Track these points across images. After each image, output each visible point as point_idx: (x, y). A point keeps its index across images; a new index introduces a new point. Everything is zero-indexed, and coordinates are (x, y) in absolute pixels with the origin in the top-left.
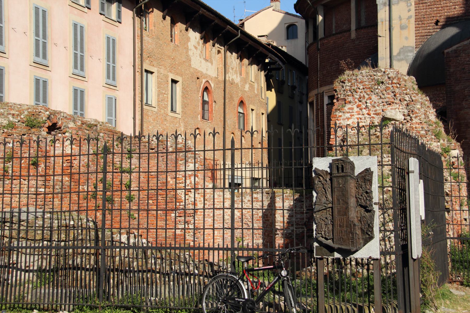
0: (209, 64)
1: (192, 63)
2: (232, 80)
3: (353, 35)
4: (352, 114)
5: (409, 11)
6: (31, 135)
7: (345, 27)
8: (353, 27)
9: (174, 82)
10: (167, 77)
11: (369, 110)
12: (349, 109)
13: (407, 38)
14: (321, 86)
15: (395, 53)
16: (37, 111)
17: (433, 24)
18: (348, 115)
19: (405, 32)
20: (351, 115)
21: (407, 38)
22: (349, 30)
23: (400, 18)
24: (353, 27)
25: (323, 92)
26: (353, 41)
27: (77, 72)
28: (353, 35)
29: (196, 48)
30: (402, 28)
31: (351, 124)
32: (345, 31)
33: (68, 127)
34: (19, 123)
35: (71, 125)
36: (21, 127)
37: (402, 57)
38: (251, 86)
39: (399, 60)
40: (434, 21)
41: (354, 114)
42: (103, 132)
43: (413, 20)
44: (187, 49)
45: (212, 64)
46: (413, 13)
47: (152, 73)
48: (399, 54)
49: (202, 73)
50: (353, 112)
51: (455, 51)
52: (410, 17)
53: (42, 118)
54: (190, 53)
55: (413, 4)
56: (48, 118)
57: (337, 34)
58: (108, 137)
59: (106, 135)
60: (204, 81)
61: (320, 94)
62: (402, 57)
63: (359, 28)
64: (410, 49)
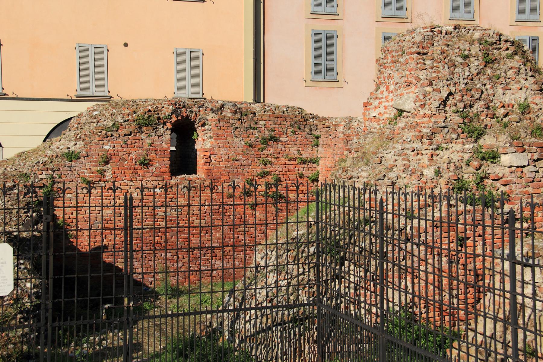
4: (381, 101)
6: (138, 135)
16: (159, 106)
20: (379, 104)
31: (377, 116)
33: (207, 120)
34: (126, 123)
35: (211, 116)
36: (129, 127)
41: (382, 100)
42: (266, 119)
50: (382, 98)
53: (165, 114)
56: (172, 113)
58: (274, 124)
59: (272, 123)
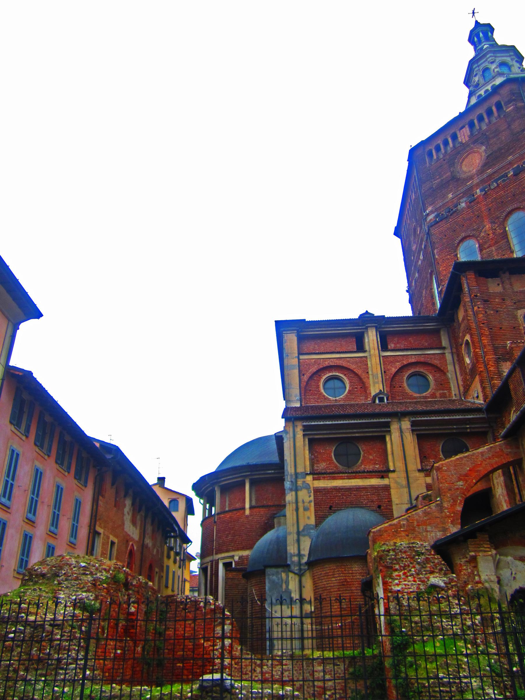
0: (135, 529)
1: (125, 526)
2: (147, 544)
3: (247, 512)
5: (310, 496)
7: (238, 505)
8: (247, 506)
9: (113, 543)
10: (108, 538)
11: (414, 578)
12: (397, 575)
13: (309, 518)
14: (216, 554)
15: (301, 528)
17: (328, 509)
18: (397, 581)
19: (307, 513)
22: (244, 508)
23: (303, 502)
24: (247, 506)
25: (218, 560)
26: (247, 517)
27: (53, 529)
28: (247, 512)
29: (128, 514)
30: (306, 509)
32: (240, 509)
38: (158, 551)
39: (304, 536)
43: (313, 504)
44: (123, 514)
45: (136, 528)
46: (312, 498)
47: (99, 534)
48: (303, 530)
49: (129, 535)
51: (380, 530)
52: (310, 502)
54: (125, 518)
55: (312, 492)
57: (230, 511)
60: (131, 543)
61: (215, 560)
62: (305, 533)
63: (251, 508)
64: (312, 526)
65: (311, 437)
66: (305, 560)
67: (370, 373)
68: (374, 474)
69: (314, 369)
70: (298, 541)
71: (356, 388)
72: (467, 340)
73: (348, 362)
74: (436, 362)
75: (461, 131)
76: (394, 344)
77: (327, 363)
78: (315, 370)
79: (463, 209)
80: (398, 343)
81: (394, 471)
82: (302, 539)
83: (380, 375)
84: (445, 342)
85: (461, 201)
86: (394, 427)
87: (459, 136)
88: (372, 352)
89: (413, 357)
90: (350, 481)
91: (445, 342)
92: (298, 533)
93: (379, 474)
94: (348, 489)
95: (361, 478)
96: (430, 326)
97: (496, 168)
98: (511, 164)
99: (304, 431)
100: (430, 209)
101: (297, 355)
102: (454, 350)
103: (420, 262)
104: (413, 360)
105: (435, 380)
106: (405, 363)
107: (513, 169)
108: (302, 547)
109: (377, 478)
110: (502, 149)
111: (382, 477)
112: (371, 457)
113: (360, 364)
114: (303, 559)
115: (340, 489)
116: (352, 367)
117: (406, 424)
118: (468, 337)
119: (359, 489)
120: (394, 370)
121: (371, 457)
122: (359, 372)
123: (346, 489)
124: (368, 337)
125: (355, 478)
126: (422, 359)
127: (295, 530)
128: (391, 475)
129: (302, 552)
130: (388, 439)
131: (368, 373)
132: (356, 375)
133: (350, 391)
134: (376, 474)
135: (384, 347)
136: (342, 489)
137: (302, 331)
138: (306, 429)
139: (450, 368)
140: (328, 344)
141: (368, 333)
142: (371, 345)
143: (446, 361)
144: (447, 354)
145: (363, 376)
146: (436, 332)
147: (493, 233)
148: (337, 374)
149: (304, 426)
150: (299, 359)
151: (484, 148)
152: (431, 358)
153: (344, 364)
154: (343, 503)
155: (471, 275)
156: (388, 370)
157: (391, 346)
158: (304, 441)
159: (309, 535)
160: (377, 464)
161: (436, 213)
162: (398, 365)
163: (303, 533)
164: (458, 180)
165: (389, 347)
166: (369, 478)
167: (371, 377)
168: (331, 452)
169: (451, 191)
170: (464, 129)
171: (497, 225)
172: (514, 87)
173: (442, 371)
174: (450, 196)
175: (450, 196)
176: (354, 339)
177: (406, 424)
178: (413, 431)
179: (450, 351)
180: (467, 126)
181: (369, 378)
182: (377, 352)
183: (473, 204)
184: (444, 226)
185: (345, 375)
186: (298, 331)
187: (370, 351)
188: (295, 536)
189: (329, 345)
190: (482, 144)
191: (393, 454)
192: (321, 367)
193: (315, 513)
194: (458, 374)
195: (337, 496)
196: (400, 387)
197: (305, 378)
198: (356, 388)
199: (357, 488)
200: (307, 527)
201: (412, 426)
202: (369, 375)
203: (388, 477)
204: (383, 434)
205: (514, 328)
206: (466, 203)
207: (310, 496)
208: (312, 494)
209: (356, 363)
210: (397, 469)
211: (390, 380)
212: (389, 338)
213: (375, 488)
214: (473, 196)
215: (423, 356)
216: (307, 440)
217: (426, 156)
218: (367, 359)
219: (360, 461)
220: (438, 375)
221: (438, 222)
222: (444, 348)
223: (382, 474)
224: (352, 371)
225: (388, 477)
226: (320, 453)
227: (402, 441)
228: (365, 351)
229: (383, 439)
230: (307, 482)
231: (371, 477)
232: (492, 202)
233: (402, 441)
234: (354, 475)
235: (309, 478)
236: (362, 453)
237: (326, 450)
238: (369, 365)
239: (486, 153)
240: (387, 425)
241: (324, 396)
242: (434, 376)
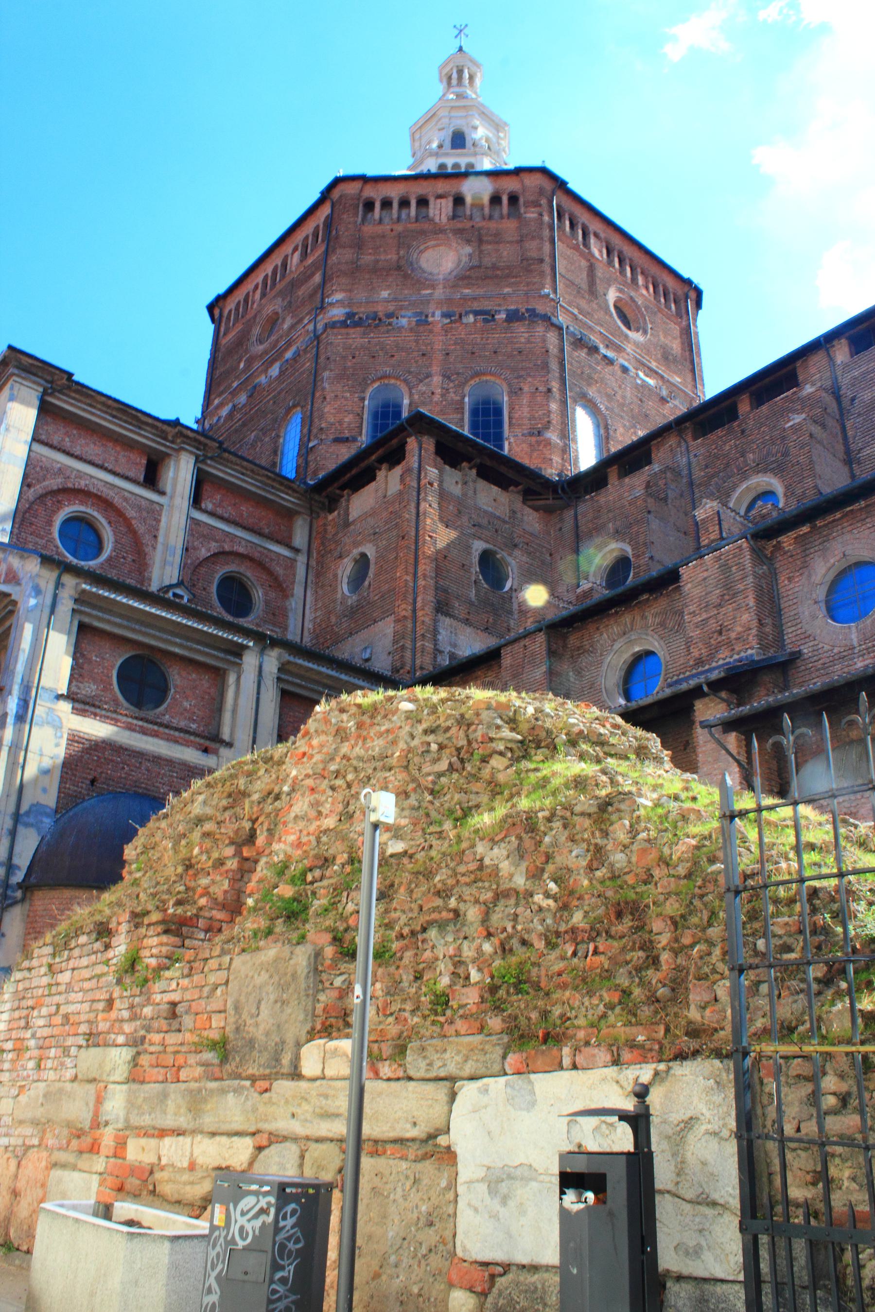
15: (24, 808)
17: (88, 782)
21: (45, 790)
37: (31, 820)
39: (27, 825)
40: (90, 777)
48: (28, 813)
55: (65, 736)
62: (31, 820)
64: (48, 810)
65: (86, 620)
66: (18, 877)
67: (161, 539)
68: (192, 738)
69: (54, 483)
70: (13, 833)
71: (124, 558)
72: (364, 555)
73: (126, 500)
74: (279, 571)
75: (439, 201)
76: (214, 504)
77: (82, 484)
78: (55, 488)
79: (400, 328)
80: (220, 506)
81: (230, 745)
82: (21, 830)
83: (179, 552)
84: (300, 538)
85: (403, 313)
86: (250, 660)
87: (431, 206)
88: (178, 501)
89: (243, 543)
90: (145, 738)
91: (300, 538)
92: (17, 817)
93: (202, 741)
94: (138, 752)
95: (168, 740)
96: (288, 499)
97: (480, 292)
98: (505, 297)
99: (76, 601)
100: (338, 296)
101: (29, 439)
102: (313, 563)
103: (263, 379)
104: (241, 550)
105: (267, 603)
106: (227, 548)
107: (507, 310)
108: (17, 849)
109: (197, 749)
110: (498, 269)
111: (206, 750)
112: (186, 704)
113: (145, 514)
114: (14, 874)
115: (121, 747)
116: (131, 513)
117: (272, 661)
118: (370, 550)
119: (157, 759)
120: (204, 553)
121: (186, 704)
122: (141, 529)
123: (134, 751)
124: (177, 470)
125: (155, 735)
126: (257, 555)
127: (12, 808)
128: (224, 751)
129: (16, 861)
130: (232, 678)
131: (155, 537)
132: (133, 532)
133: (110, 559)
134: (198, 739)
135: (196, 500)
136: (126, 749)
137: (51, 395)
138: (81, 599)
139: (298, 590)
140: (92, 446)
141: (178, 461)
142: (179, 488)
143: (294, 575)
144: (299, 564)
145: (147, 539)
146: (289, 515)
147: (443, 395)
148: (95, 514)
149: (84, 591)
150: (30, 450)
151: (468, 249)
152: (272, 560)
153: (117, 501)
154: (120, 777)
155: (429, 444)
156: (195, 549)
157: (208, 505)
158: (71, 622)
159: (37, 826)
160: (194, 721)
161: (347, 310)
162: (214, 547)
163: (25, 819)
164: (406, 276)
165: (203, 506)
166: (182, 744)
167: (160, 547)
168: (113, 667)
169: (389, 287)
170: (443, 201)
171: (451, 385)
172: (548, 185)
173: (283, 590)
174: (385, 294)
175: (385, 294)
176: (144, 462)
177: (272, 661)
178: (278, 679)
179: (305, 560)
180: (451, 199)
181: (154, 548)
182: (186, 504)
183: (421, 328)
184: (356, 338)
185: (110, 523)
186: (45, 390)
187: (172, 497)
188: (9, 823)
189: (92, 448)
190: (468, 242)
191: (234, 711)
192: (70, 485)
193: (61, 782)
194: (307, 607)
195: (112, 761)
196: (205, 589)
197: (31, 494)
198: (124, 558)
199: (154, 757)
200: (37, 809)
201: (279, 670)
202: (156, 542)
203: (216, 752)
204: (225, 667)
205: (463, 565)
206: (409, 323)
207: (57, 745)
208: (64, 742)
209: (140, 509)
210: (237, 744)
211: (192, 568)
212: (207, 488)
213: (190, 766)
214: (427, 316)
215: (259, 549)
216: (76, 623)
217: (361, 205)
218: (161, 510)
219: (165, 705)
220: (273, 595)
221: (347, 326)
222: (297, 551)
223: (208, 743)
224: (127, 522)
225: (216, 752)
226: (90, 661)
227: (258, 693)
228: (162, 493)
229: (218, 675)
230: (60, 714)
231: (187, 744)
232: (455, 344)
233: (258, 693)
234: (156, 728)
235: (65, 707)
236: (172, 691)
237: (103, 659)
238: (163, 524)
239: (470, 260)
240: (238, 651)
241: (57, 547)
242: (266, 594)
